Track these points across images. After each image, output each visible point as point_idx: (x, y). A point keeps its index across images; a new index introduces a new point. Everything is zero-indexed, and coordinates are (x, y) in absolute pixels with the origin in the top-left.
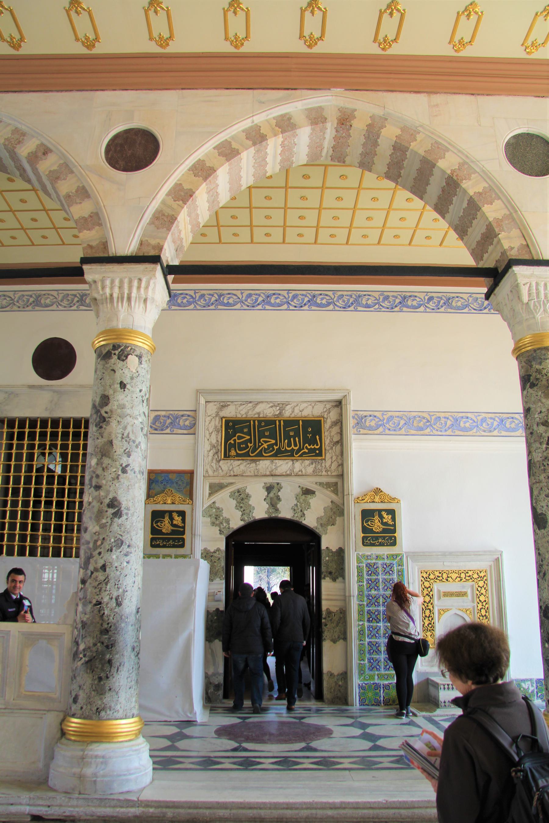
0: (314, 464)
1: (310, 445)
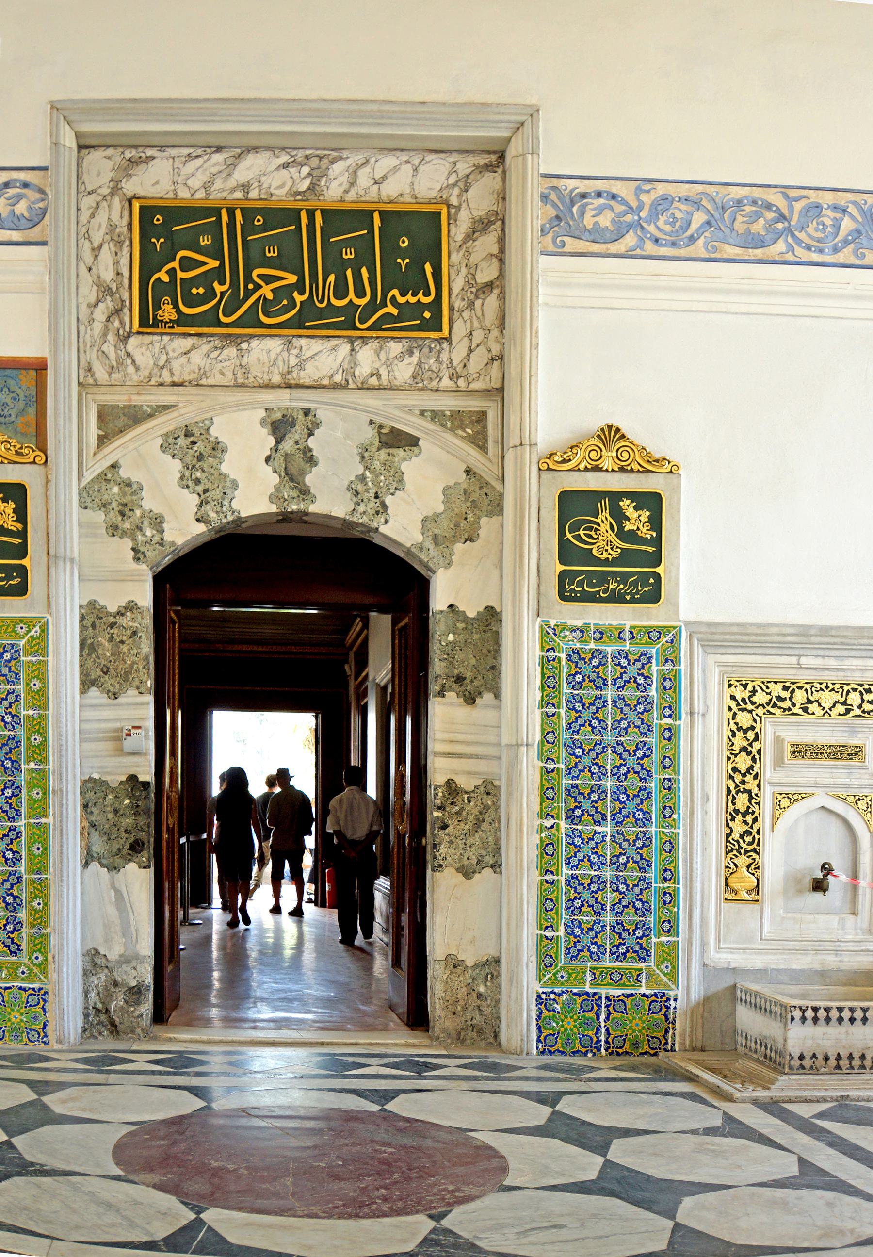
0: (417, 353)
1: (403, 294)
